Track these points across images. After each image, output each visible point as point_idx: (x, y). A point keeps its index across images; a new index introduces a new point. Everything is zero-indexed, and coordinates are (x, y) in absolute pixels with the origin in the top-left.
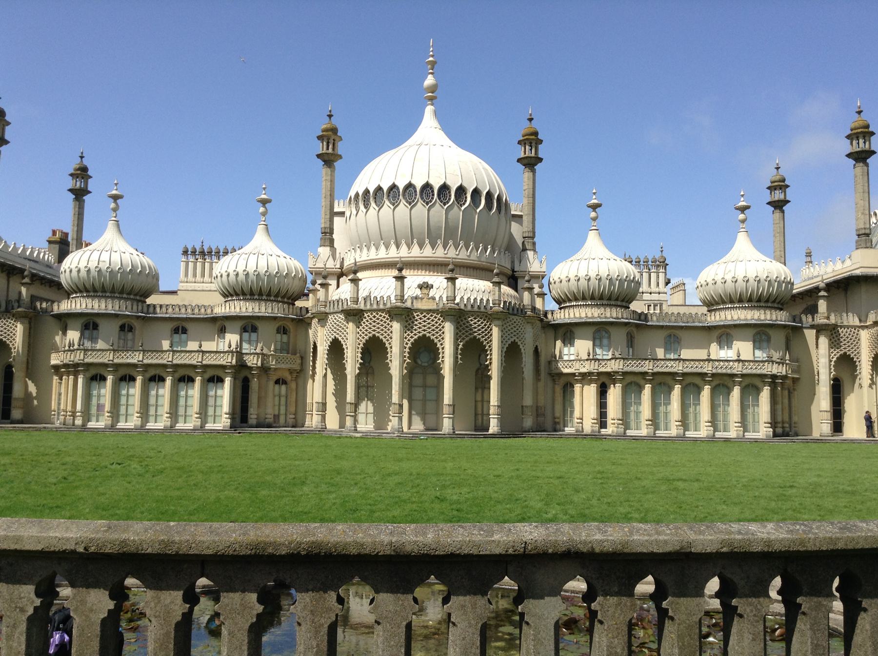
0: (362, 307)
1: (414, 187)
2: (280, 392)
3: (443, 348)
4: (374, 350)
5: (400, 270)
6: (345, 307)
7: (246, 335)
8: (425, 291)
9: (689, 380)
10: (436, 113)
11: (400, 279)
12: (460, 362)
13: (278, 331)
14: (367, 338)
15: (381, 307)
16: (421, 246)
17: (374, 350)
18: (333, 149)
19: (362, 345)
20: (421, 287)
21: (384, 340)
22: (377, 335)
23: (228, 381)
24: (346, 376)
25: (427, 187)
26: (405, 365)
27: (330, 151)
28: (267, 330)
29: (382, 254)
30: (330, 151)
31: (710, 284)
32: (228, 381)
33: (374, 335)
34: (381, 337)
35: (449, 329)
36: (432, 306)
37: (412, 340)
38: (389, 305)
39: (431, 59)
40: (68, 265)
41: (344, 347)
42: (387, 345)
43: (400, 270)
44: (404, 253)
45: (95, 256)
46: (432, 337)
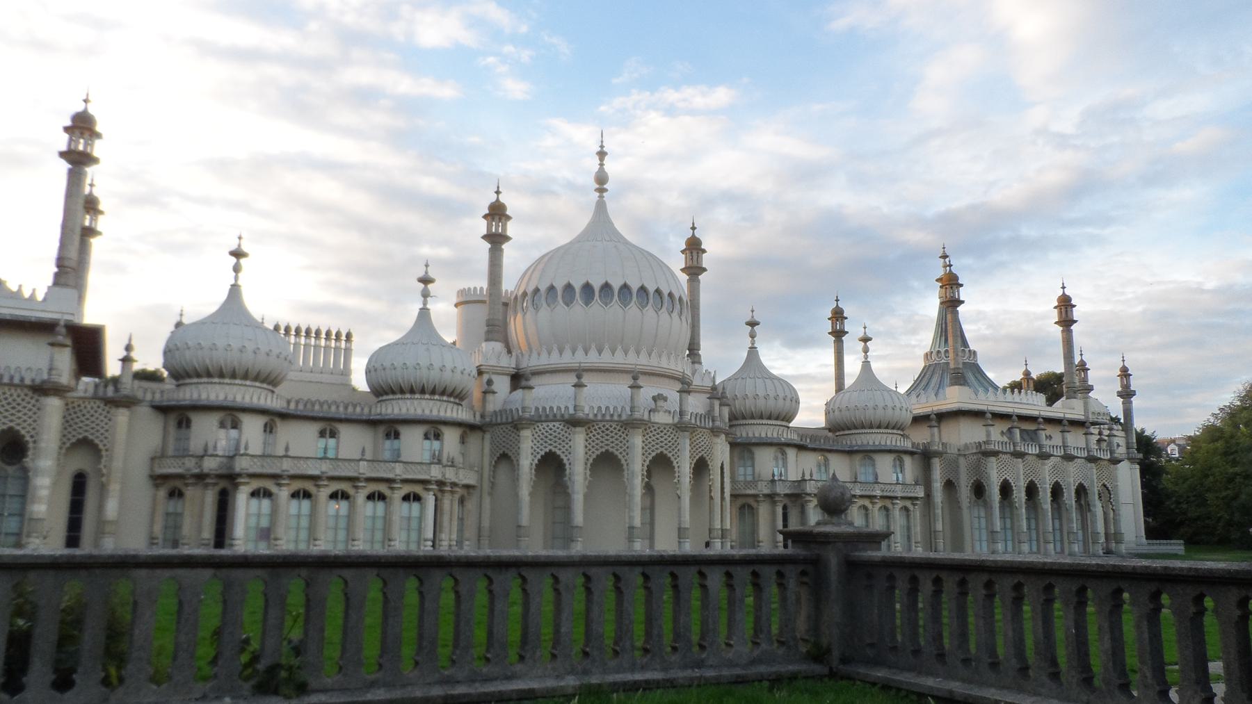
0: (591, 416)
2: (260, 508)
5: (635, 378)
6: (567, 417)
7: (427, 443)
8: (660, 403)
9: (861, 502)
11: (635, 387)
13: (426, 437)
15: (616, 418)
19: (591, 460)
20: (654, 399)
21: (620, 456)
23: (430, 500)
28: (451, 437)
32: (430, 500)
34: (617, 453)
35: (685, 444)
37: (650, 458)
38: (624, 417)
41: (565, 461)
42: (623, 462)
43: (635, 378)
44: (580, 358)
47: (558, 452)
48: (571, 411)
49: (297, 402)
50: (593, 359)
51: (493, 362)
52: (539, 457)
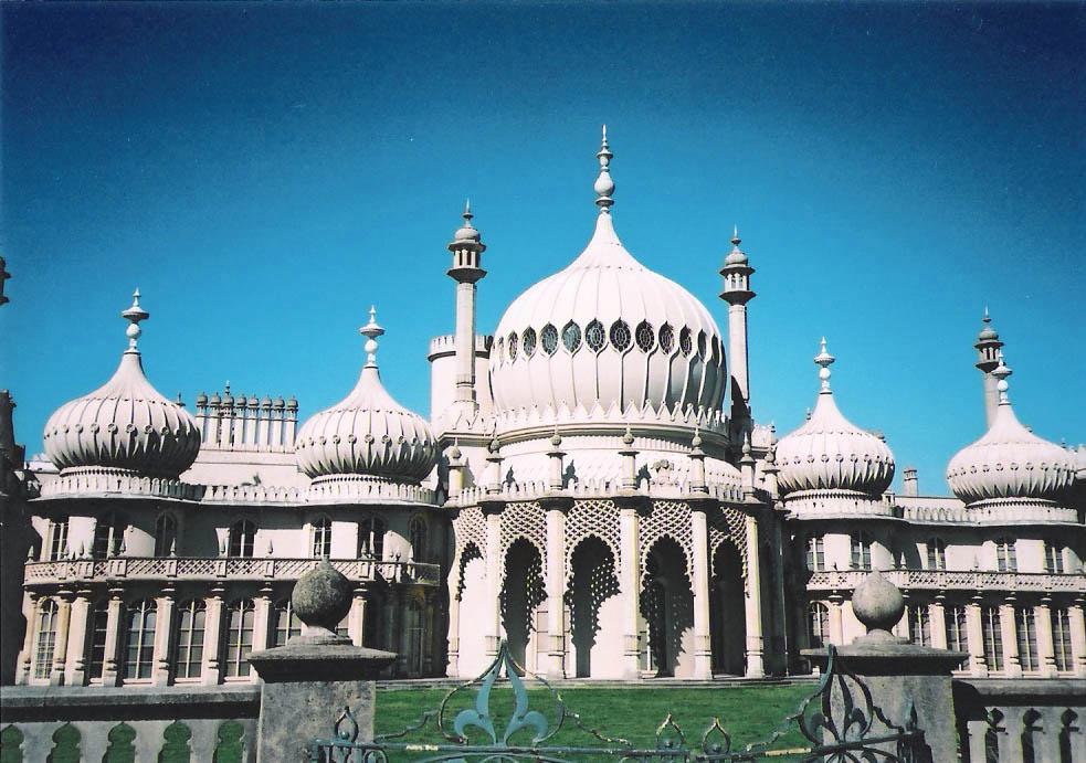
1: (626, 326)
3: (692, 555)
4: (592, 560)
10: (617, 226)
12: (713, 574)
14: (581, 539)
16: (606, 409)
17: (592, 560)
18: (477, 265)
21: (609, 543)
22: (597, 535)
24: (692, 595)
25: (619, 326)
26: (642, 579)
27: (473, 266)
29: (599, 417)
30: (473, 266)
31: (968, 473)
33: (592, 536)
34: (603, 538)
36: (675, 494)
39: (605, 151)
40: (63, 420)
42: (614, 550)
45: (125, 408)
46: (677, 539)
47: (531, 539)
48: (548, 488)
49: (215, 489)
50: (565, 418)
51: (463, 428)
52: (508, 545)
